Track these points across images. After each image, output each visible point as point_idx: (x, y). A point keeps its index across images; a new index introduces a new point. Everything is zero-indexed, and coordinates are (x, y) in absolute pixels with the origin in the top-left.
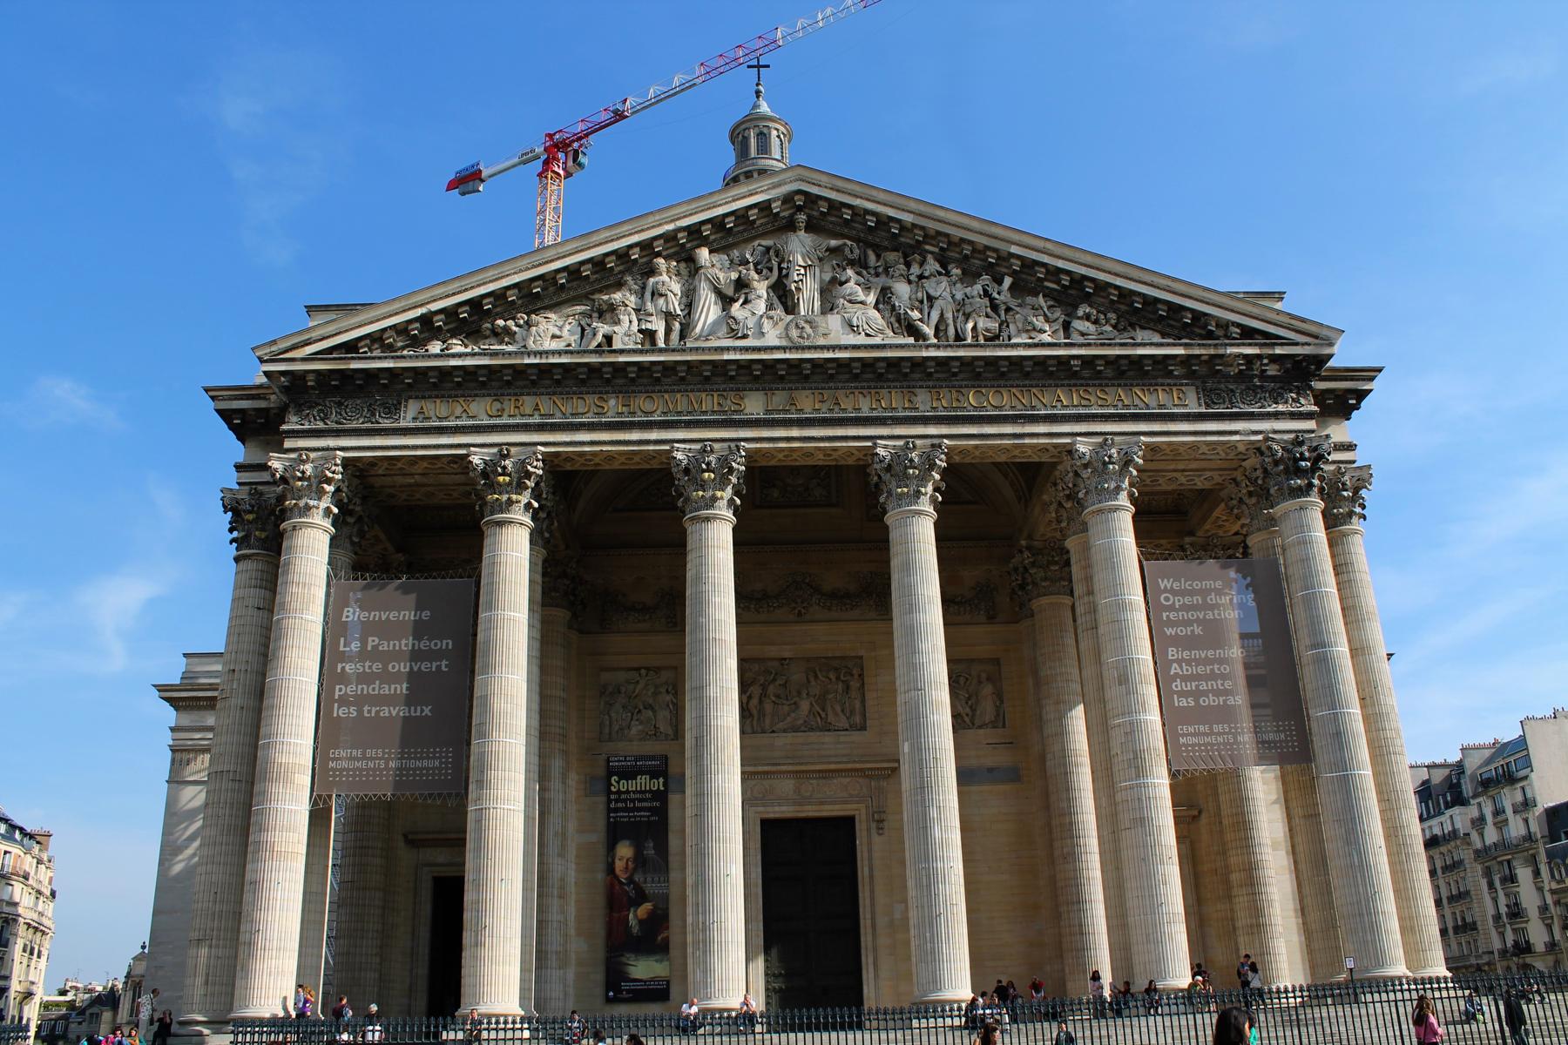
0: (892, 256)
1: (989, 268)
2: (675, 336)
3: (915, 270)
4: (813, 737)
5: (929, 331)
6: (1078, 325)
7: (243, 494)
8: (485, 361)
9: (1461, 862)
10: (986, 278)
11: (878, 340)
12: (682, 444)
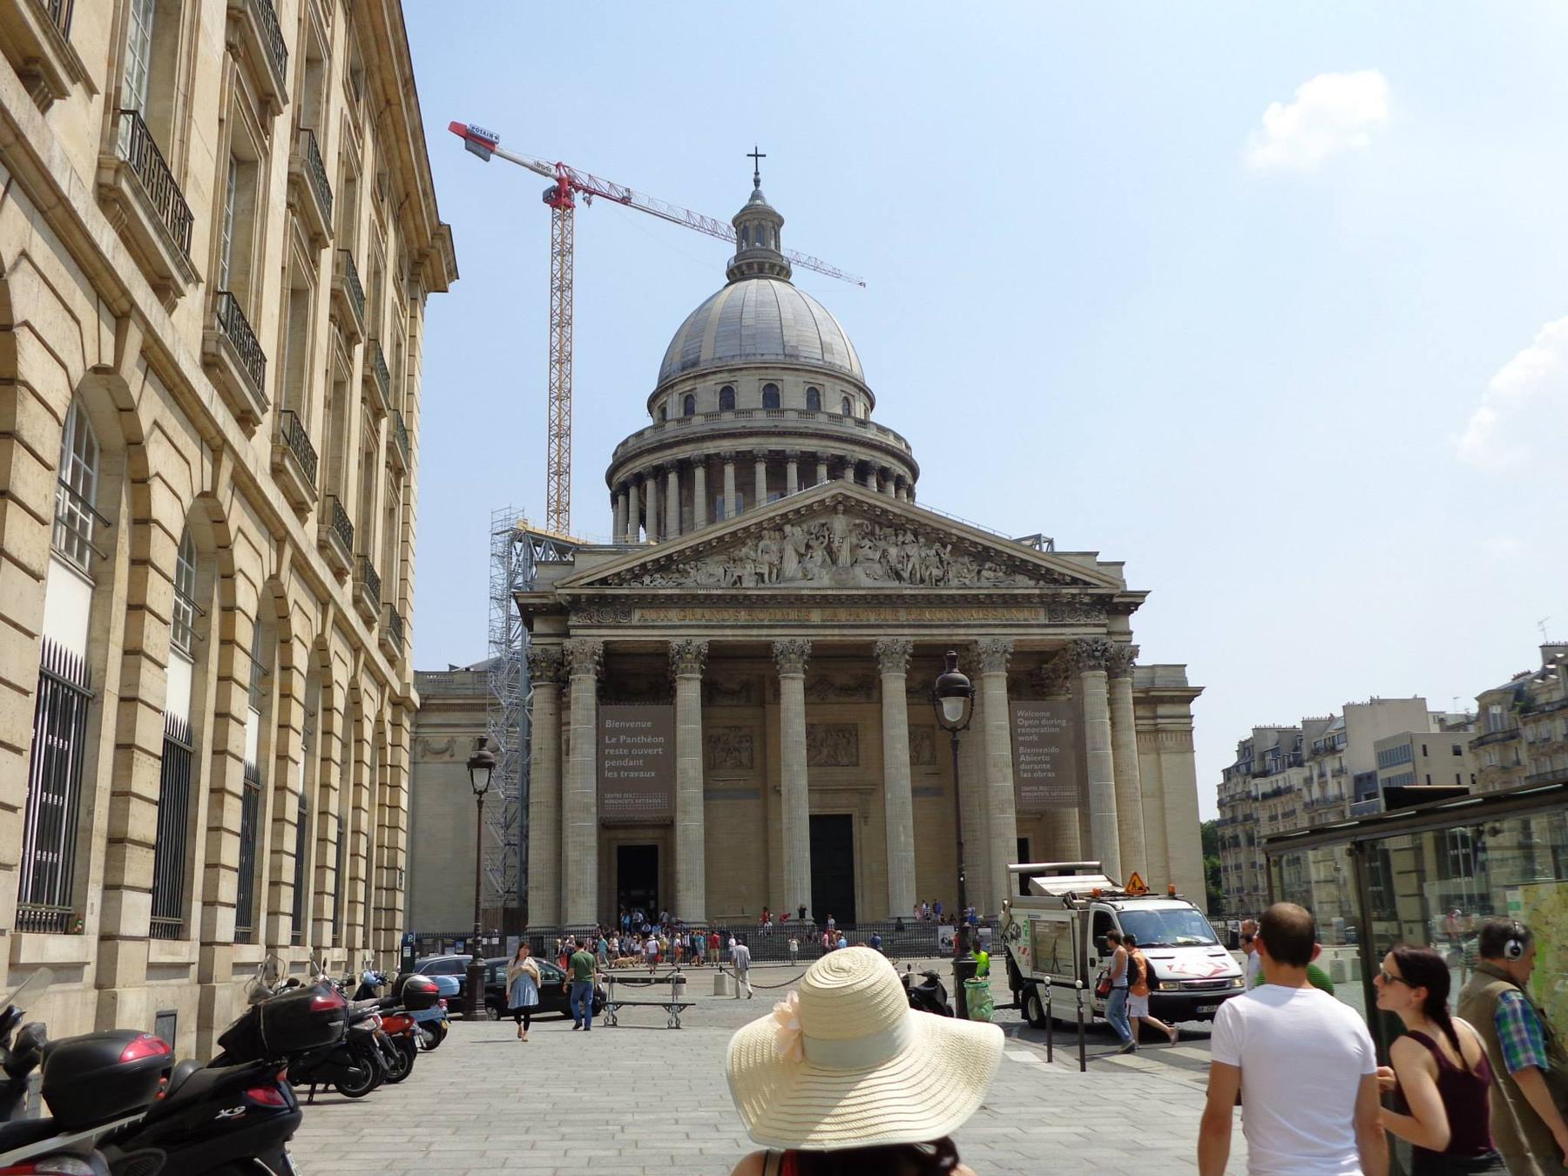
0: (889, 531)
1: (940, 540)
2: (774, 576)
3: (900, 538)
4: (829, 769)
5: (906, 575)
6: (984, 573)
7: (538, 650)
8: (677, 591)
9: (1294, 812)
10: (937, 545)
11: (879, 584)
12: (781, 638)
